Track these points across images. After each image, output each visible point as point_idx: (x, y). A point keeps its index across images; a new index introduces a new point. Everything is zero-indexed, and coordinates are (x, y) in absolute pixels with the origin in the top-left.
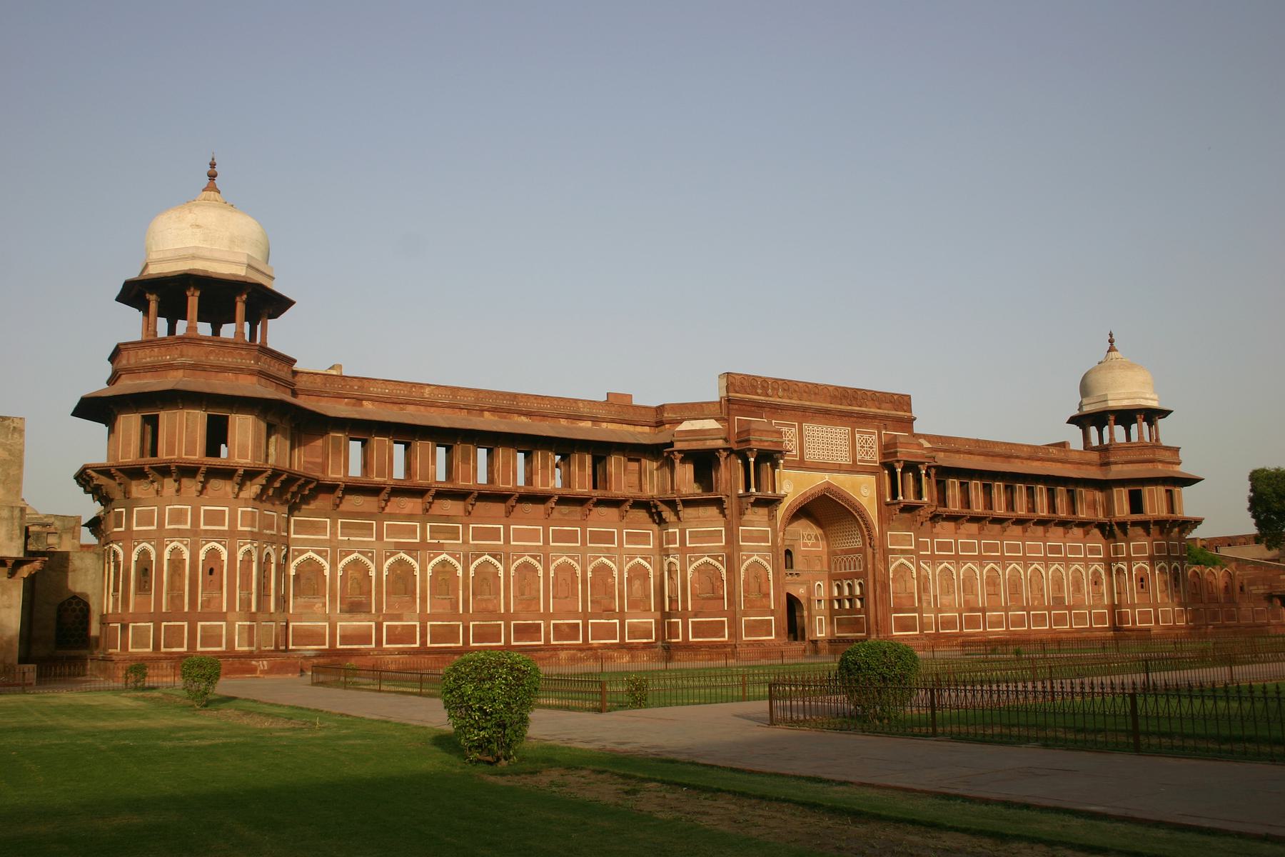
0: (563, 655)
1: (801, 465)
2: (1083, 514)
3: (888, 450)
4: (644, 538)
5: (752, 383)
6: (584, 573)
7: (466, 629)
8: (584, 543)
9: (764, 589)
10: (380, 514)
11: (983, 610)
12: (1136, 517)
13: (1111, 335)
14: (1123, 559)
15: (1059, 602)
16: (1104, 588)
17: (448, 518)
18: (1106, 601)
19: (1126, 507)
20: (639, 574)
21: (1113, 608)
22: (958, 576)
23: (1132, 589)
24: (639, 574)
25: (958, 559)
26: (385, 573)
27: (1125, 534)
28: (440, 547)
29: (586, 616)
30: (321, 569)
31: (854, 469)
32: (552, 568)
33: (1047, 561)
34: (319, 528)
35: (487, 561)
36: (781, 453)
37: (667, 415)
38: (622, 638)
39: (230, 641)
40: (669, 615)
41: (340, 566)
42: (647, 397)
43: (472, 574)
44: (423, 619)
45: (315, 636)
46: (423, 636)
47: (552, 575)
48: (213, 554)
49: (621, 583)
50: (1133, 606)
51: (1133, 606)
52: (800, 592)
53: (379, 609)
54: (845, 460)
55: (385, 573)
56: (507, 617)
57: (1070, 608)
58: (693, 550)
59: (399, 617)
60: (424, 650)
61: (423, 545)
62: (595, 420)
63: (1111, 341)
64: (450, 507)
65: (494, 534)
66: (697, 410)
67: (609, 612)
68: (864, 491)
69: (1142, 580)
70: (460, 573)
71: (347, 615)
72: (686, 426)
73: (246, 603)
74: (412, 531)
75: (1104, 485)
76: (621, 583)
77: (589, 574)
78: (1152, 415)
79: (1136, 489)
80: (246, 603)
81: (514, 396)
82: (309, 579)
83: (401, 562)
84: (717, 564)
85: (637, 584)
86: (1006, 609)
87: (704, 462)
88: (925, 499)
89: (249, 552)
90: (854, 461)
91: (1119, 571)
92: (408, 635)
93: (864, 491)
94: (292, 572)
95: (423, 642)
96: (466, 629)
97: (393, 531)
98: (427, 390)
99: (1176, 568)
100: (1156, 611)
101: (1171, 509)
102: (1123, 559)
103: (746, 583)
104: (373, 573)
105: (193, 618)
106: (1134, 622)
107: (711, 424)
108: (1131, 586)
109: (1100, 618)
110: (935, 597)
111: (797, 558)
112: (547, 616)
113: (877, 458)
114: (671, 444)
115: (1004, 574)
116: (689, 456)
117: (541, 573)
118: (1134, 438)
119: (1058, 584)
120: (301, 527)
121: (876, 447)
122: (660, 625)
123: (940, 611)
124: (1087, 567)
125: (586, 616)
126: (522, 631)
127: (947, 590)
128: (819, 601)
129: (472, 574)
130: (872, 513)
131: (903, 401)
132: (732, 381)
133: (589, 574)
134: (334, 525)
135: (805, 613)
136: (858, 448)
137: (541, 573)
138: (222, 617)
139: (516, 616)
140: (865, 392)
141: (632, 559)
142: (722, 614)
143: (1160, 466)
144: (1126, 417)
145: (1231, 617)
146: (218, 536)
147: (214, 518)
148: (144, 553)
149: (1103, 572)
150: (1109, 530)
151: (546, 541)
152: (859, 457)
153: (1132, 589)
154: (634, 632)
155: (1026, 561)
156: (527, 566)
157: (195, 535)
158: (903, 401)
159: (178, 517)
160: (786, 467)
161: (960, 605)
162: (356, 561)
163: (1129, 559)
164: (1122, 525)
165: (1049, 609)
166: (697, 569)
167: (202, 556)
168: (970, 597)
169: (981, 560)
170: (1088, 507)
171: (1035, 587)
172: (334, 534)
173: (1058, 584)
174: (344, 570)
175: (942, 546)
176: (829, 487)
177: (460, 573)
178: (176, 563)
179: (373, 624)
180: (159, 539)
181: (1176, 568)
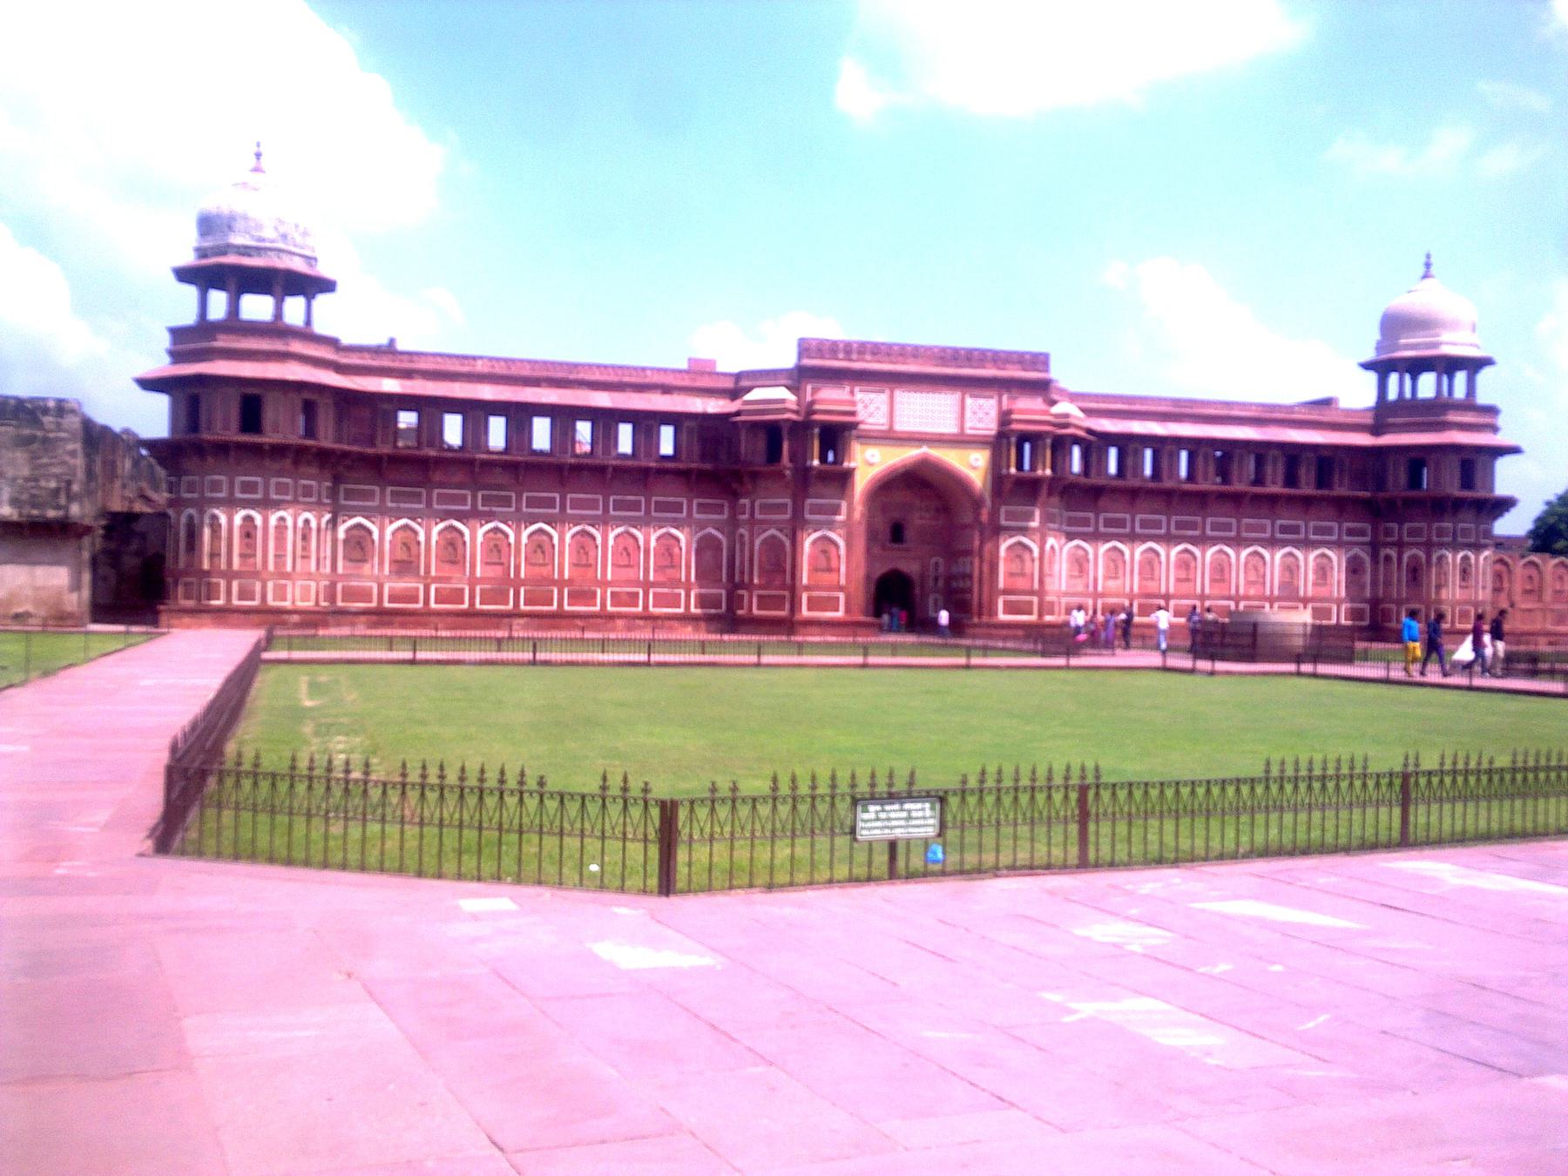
0: (620, 623)
1: (889, 437)
2: (1341, 490)
3: (1005, 418)
4: (718, 509)
5: (833, 348)
6: (647, 542)
7: (517, 594)
8: (648, 512)
9: (834, 564)
10: (426, 483)
12: (1413, 493)
16: (1368, 578)
17: (499, 487)
18: (1368, 593)
19: (1403, 478)
21: (1375, 603)
26: (434, 538)
30: (370, 532)
31: (961, 441)
34: (368, 495)
36: (854, 425)
37: (744, 383)
40: (737, 586)
42: (730, 363)
44: (473, 582)
45: (364, 595)
46: (472, 598)
47: (611, 542)
49: (688, 552)
50: (1399, 603)
52: (911, 567)
54: (949, 427)
55: (434, 538)
56: (561, 583)
58: (762, 522)
59: (447, 579)
60: (471, 614)
62: (666, 389)
63: (1428, 265)
64: (499, 477)
67: (676, 583)
68: (973, 466)
70: (512, 540)
71: (394, 577)
72: (756, 394)
74: (463, 500)
78: (1474, 365)
79: (1417, 458)
81: (576, 366)
83: (452, 528)
84: (784, 538)
85: (708, 554)
87: (772, 432)
89: (282, 519)
90: (962, 428)
91: (1388, 558)
92: (457, 596)
95: (472, 603)
96: (517, 594)
97: (443, 499)
98: (480, 363)
101: (1467, 481)
103: (812, 557)
105: (230, 575)
107: (781, 393)
108: (1399, 577)
110: (1096, 580)
111: (909, 534)
112: (604, 584)
114: (738, 413)
116: (754, 424)
119: (1291, 569)
120: (349, 495)
121: (994, 414)
123: (1102, 595)
127: (1112, 574)
128: (936, 579)
132: (804, 348)
133: (653, 544)
135: (917, 591)
136: (968, 414)
138: (255, 575)
139: (570, 582)
140: (983, 352)
141: (702, 528)
142: (783, 587)
144: (1448, 366)
148: (191, 517)
149: (1367, 559)
151: (606, 510)
152: (968, 424)
153: (1399, 581)
159: (216, 486)
160: (858, 437)
162: (406, 527)
164: (1391, 502)
166: (765, 542)
172: (383, 500)
174: (394, 534)
175: (1108, 523)
177: (512, 540)
178: (281, 527)
179: (421, 587)
180: (202, 504)
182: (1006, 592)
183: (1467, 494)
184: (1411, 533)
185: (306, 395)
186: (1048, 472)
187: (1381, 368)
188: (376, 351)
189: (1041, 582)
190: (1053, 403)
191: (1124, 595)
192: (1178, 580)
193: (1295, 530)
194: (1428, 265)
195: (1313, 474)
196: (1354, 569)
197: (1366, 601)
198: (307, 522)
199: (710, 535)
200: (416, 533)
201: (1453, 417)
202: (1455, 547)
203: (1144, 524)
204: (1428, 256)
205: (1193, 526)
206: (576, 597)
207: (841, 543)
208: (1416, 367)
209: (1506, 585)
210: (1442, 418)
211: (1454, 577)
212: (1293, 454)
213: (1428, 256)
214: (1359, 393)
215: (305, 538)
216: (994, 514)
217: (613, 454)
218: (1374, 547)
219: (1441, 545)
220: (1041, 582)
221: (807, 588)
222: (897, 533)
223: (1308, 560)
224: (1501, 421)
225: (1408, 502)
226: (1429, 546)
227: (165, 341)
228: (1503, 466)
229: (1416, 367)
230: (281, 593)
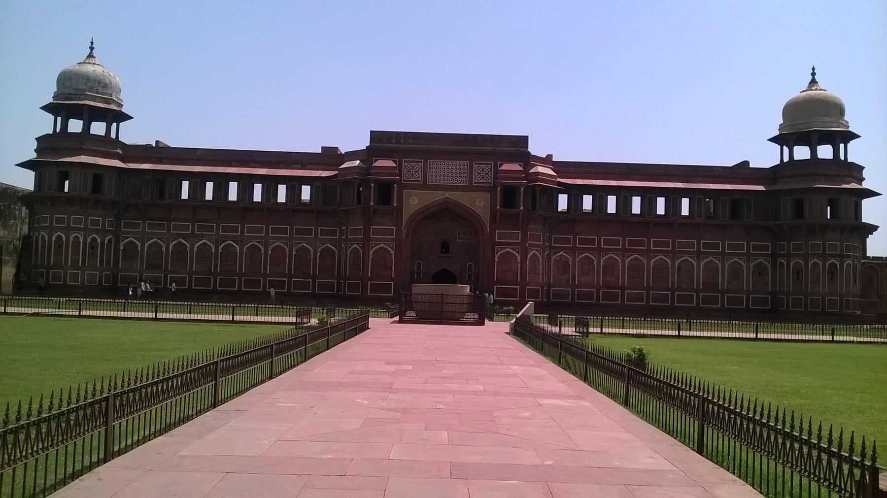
1: (424, 186)
4: (334, 233)
8: (291, 234)
11: (623, 288)
20: (327, 253)
22: (599, 263)
23: (788, 279)
24: (327, 253)
25: (599, 251)
28: (202, 236)
29: (290, 276)
31: (470, 188)
32: (270, 248)
33: (699, 255)
35: (229, 244)
38: (314, 289)
39: (65, 280)
41: (146, 245)
43: (220, 251)
47: (270, 252)
48: (59, 237)
49: (315, 258)
53: (166, 268)
54: (463, 181)
57: (723, 292)
61: (193, 234)
63: (813, 74)
65: (235, 229)
66: (351, 155)
67: (307, 275)
68: (480, 204)
69: (798, 273)
70: (213, 250)
72: (346, 165)
73: (75, 262)
74: (187, 228)
76: (315, 258)
77: (294, 253)
80: (75, 262)
82: (131, 251)
83: (181, 242)
86: (648, 289)
88: (522, 208)
89: (77, 237)
90: (471, 182)
91: (781, 264)
93: (480, 204)
94: (122, 248)
95: (190, 285)
97: (176, 227)
99: (833, 265)
100: (806, 298)
104: (164, 249)
106: (788, 306)
110: (574, 277)
112: (265, 275)
113: (491, 181)
115: (648, 263)
117: (263, 251)
120: (127, 225)
121: (491, 174)
122: (338, 283)
125: (290, 276)
126: (248, 283)
128: (470, 276)
129: (220, 251)
130: (486, 217)
131: (524, 140)
132: (374, 135)
133: (294, 253)
134: (144, 223)
136: (475, 174)
137: (263, 251)
146: (61, 229)
147: (59, 220)
149: (769, 266)
153: (788, 279)
154: (322, 286)
155: (674, 254)
156: (254, 246)
157: (51, 230)
158: (524, 140)
162: (156, 242)
167: (54, 239)
169: (624, 252)
172: (144, 228)
174: (149, 247)
176: (447, 201)
177: (213, 250)
181: (833, 265)
182: (498, 283)
185: (97, 171)
186: (522, 208)
188: (147, 147)
189: (523, 277)
190: (534, 166)
193: (716, 246)
194: (813, 74)
196: (760, 271)
198: (94, 239)
199: (329, 248)
200: (161, 247)
204: (813, 69)
205: (641, 243)
206: (248, 283)
207: (393, 253)
208: (812, 139)
213: (813, 69)
214: (767, 157)
215: (93, 248)
216: (492, 233)
217: (272, 201)
218: (774, 257)
219: (814, 255)
220: (523, 277)
221: (371, 279)
222: (445, 247)
224: (865, 174)
226: (806, 257)
227: (35, 145)
228: (866, 203)
230: (75, 277)
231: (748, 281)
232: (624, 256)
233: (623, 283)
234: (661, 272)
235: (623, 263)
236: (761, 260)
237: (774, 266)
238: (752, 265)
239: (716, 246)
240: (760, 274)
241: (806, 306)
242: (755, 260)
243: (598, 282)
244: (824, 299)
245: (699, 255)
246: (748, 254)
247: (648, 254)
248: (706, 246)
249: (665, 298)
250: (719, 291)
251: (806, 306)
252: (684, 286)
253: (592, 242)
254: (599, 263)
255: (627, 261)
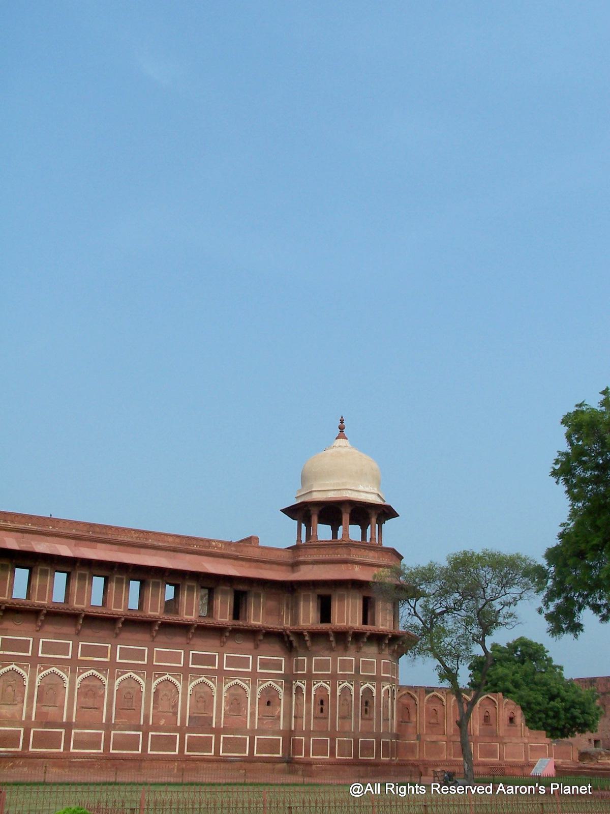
11: (68, 726)
12: (325, 626)
13: (342, 421)
14: (303, 676)
15: (201, 722)
21: (289, 735)
22: (32, 682)
23: (308, 713)
25: (34, 661)
27: (307, 648)
51: (308, 734)
57: (218, 732)
63: (342, 429)
69: (322, 702)
75: (291, 589)
79: (325, 594)
91: (299, 689)
99: (368, 690)
100: (333, 740)
102: (303, 676)
106: (307, 753)
109: (272, 746)
115: (111, 685)
118: (340, 537)
119: (203, 699)
124: (254, 683)
143: (357, 568)
145: (492, 754)
149: (282, 691)
150: (289, 642)
153: (308, 713)
155: (151, 670)
161: (29, 717)
163: (309, 677)
164: (299, 635)
165: (182, 730)
168: (51, 710)
169: (74, 665)
170: (268, 613)
171: (164, 706)
173: (203, 699)
181: (368, 690)
183: (369, 628)
184: (321, 665)
187: (301, 512)
191: (21, 724)
192: (81, 708)
193: (210, 660)
194: (342, 429)
195: (230, 601)
196: (269, 700)
197: (278, 733)
201: (356, 555)
202: (357, 678)
203: (47, 648)
204: (342, 421)
205: (102, 652)
209: (413, 718)
210: (345, 556)
211: (355, 708)
212: (210, 583)
218: (289, 679)
219: (345, 677)
223: (220, 692)
225: (316, 635)
226: (333, 678)
229: (331, 512)
231: (253, 714)
232: (73, 671)
233: (70, 716)
234: (128, 701)
235: (72, 682)
236: (270, 682)
237: (288, 690)
238: (258, 690)
239: (210, 660)
240: (269, 703)
241: (333, 753)
242: (264, 682)
243: (29, 717)
244: (356, 742)
245: (185, 672)
246: (254, 675)
247: (111, 668)
248: (197, 659)
249: (132, 743)
250: (212, 731)
251: (333, 753)
252: (162, 722)
253: (23, 646)
254: (32, 682)
255: (78, 680)
